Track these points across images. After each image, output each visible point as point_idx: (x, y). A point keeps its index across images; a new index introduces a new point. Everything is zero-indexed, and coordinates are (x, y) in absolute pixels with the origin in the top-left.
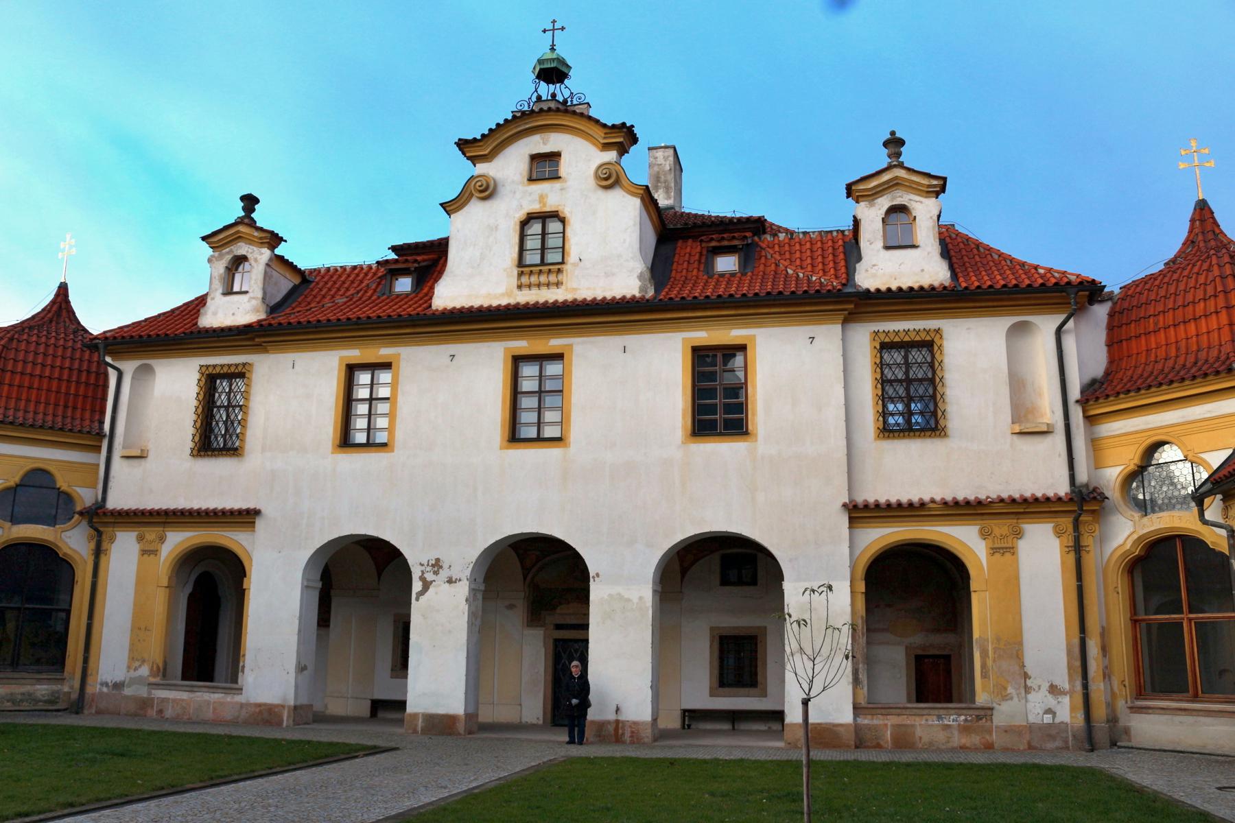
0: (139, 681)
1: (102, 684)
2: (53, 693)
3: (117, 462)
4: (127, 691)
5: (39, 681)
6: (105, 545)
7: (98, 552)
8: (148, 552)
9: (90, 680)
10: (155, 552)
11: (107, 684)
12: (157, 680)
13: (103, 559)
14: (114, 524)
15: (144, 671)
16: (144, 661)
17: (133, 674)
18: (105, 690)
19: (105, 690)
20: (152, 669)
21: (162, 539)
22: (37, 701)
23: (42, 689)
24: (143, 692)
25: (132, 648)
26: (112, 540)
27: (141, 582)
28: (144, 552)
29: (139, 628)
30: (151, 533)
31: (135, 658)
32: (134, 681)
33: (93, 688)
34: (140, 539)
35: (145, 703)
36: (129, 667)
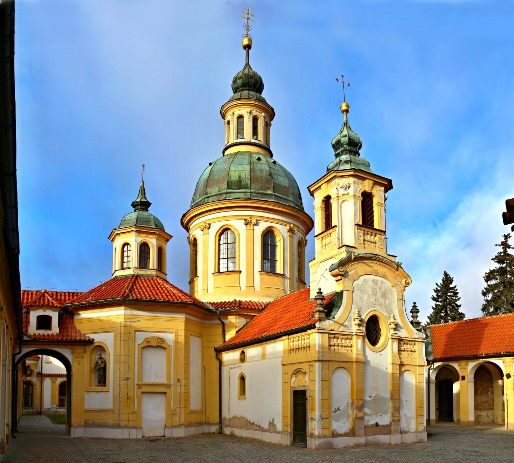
0: (54, 408)
1: (45, 409)
2: (33, 411)
3: (44, 364)
4: (51, 410)
5: (31, 409)
6: (43, 381)
7: (41, 382)
8: (53, 382)
9: (42, 408)
10: (55, 382)
11: (46, 409)
12: (58, 407)
13: (42, 384)
14: (44, 377)
15: (55, 406)
16: (54, 404)
17: (52, 406)
18: (46, 410)
19: (46, 410)
20: (56, 406)
21: (56, 380)
22: (30, 413)
23: (31, 410)
24: (55, 410)
25: (51, 401)
26: (44, 380)
27: (52, 388)
28: (52, 382)
29: (53, 397)
30: (54, 379)
31: (52, 403)
32: (52, 408)
33: (43, 410)
34: (51, 380)
35: (56, 412)
36: (51, 405)
